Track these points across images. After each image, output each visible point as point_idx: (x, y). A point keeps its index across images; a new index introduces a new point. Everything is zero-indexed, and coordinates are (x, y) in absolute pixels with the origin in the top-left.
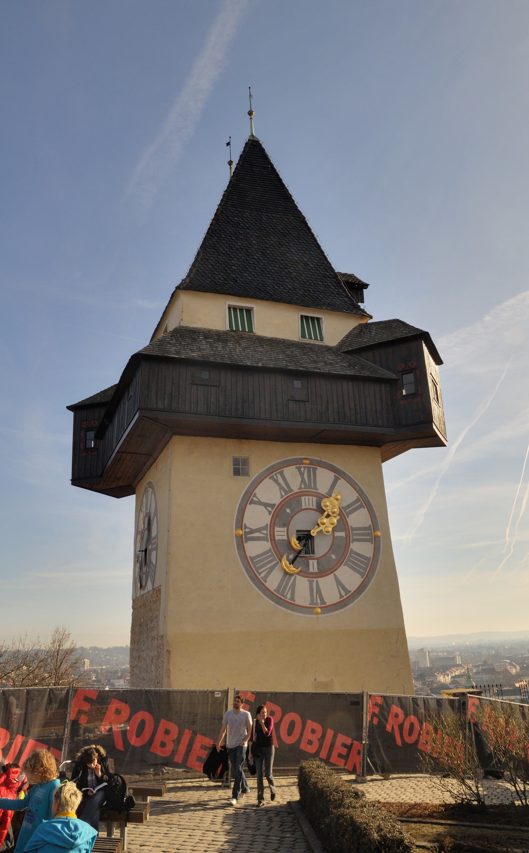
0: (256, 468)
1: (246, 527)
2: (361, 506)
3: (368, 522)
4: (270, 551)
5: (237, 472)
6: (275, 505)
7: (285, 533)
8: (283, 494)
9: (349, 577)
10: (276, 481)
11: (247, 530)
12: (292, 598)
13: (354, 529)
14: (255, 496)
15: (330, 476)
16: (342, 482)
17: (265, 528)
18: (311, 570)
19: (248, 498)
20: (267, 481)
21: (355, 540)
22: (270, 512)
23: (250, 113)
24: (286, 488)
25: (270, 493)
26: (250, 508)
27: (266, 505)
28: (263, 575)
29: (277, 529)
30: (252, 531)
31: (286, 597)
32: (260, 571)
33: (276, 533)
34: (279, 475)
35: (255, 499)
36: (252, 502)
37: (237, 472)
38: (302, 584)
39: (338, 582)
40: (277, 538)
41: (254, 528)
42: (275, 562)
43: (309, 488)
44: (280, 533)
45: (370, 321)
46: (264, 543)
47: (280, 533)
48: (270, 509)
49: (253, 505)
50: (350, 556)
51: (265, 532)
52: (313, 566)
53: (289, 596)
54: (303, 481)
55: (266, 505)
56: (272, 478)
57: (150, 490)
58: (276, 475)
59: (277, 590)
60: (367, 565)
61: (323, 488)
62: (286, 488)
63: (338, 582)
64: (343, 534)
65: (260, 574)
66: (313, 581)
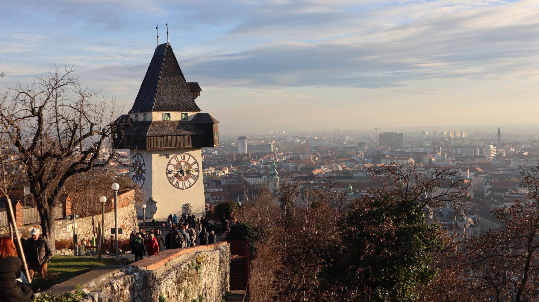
0: (171, 156)
5: (166, 158)
9: (192, 181)
15: (188, 156)
16: (191, 158)
19: (169, 164)
20: (173, 159)
23: (167, 33)
24: (177, 161)
25: (174, 162)
26: (169, 166)
37: (166, 158)
38: (181, 183)
39: (189, 182)
43: (183, 159)
45: (200, 112)
52: (183, 179)
57: (140, 156)
61: (186, 160)
62: (177, 161)
63: (189, 182)
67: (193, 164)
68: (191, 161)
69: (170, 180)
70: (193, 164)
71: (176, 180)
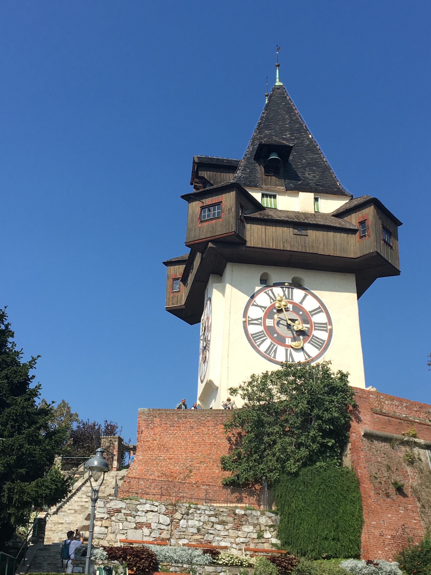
1: (249, 318)
2: (321, 311)
3: (325, 320)
4: (262, 331)
6: (266, 307)
7: (272, 323)
8: (272, 301)
10: (268, 295)
11: (250, 319)
12: (274, 357)
13: (315, 323)
14: (255, 301)
16: (309, 297)
17: (261, 319)
18: (287, 343)
21: (315, 329)
22: (263, 311)
27: (261, 307)
28: (258, 344)
29: (267, 320)
30: (253, 320)
31: (271, 356)
32: (256, 342)
33: (267, 322)
34: (270, 291)
35: (255, 303)
36: (253, 305)
40: (267, 325)
41: (254, 318)
42: (265, 338)
44: (270, 322)
46: (260, 326)
47: (270, 322)
48: (263, 309)
49: (253, 307)
50: (312, 338)
51: (260, 321)
53: (273, 356)
54: (285, 295)
55: (261, 307)
56: (266, 292)
58: (268, 291)
59: (266, 352)
60: (323, 344)
64: (308, 326)
65: (256, 343)
66: (288, 349)
67: (316, 311)
68: (310, 304)
69: (253, 340)
70: (316, 311)
71: (268, 342)
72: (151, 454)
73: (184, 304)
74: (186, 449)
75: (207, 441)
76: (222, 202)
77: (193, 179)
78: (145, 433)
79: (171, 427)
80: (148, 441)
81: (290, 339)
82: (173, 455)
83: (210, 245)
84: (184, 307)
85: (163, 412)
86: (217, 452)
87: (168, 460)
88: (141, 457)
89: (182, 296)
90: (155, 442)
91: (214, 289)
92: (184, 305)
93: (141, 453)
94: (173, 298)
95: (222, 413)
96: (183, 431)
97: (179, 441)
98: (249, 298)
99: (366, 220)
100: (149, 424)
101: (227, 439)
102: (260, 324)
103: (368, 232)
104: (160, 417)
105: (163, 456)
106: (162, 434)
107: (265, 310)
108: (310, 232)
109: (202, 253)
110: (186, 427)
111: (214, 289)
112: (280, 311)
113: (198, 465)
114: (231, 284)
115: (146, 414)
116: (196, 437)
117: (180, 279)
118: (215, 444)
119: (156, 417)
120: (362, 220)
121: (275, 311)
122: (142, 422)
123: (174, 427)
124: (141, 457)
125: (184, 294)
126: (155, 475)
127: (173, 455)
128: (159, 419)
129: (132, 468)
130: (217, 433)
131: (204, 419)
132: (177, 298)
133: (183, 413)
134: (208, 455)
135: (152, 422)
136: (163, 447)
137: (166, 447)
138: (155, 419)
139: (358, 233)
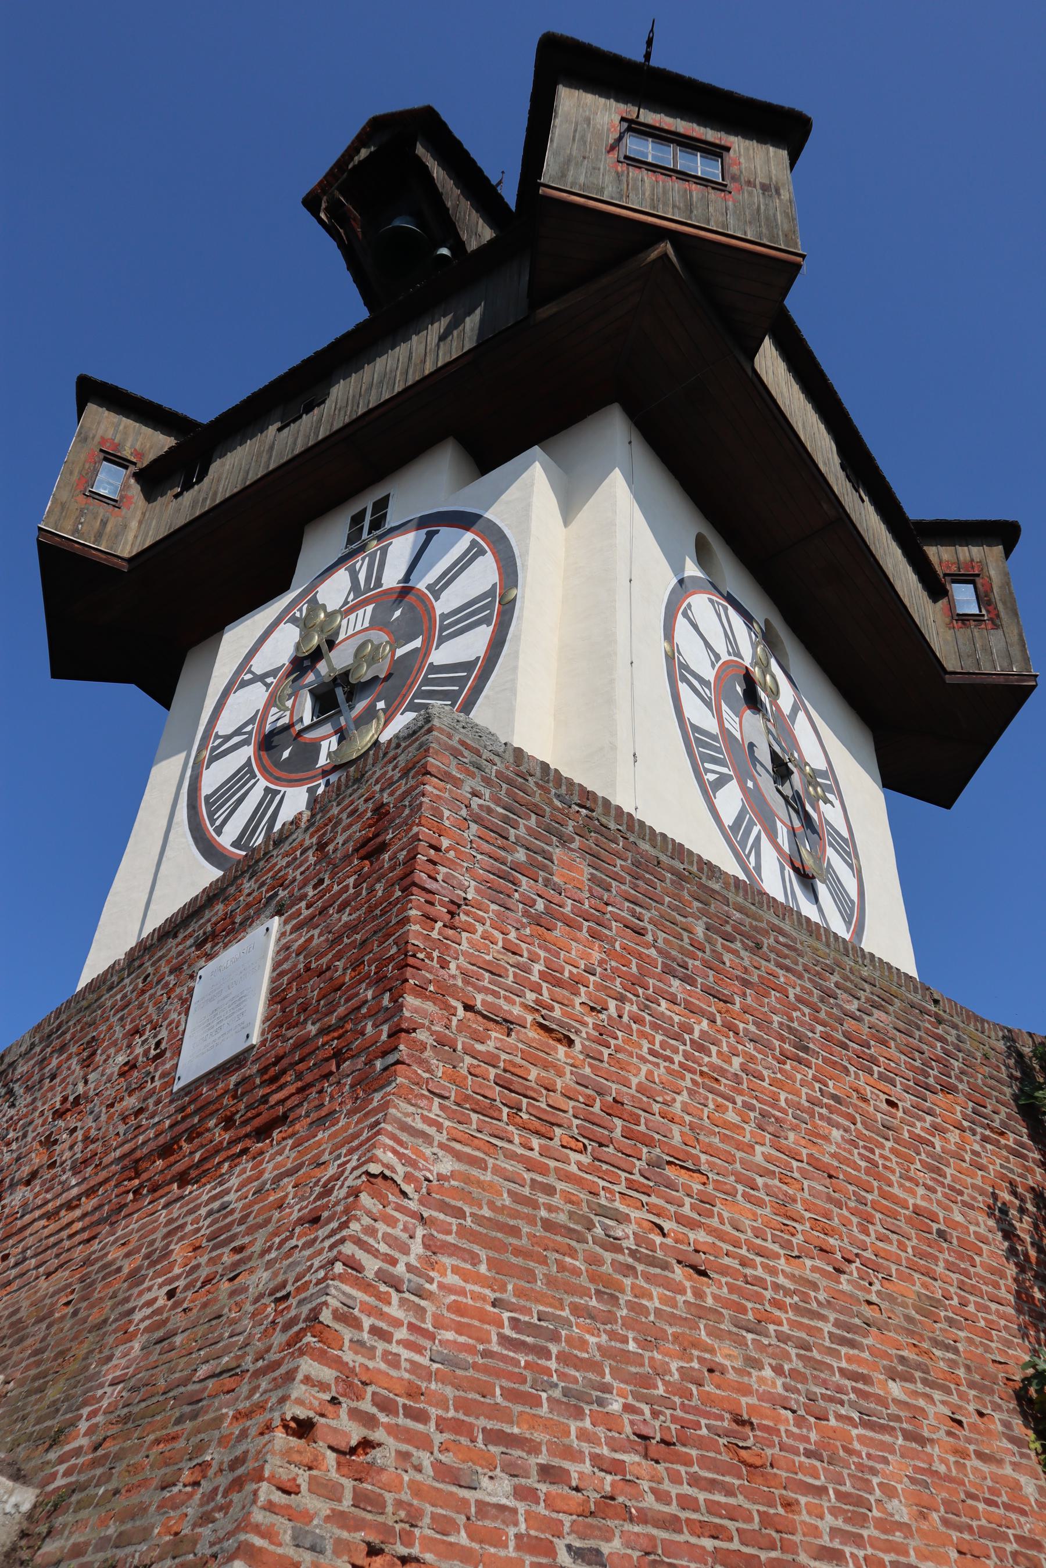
10: (719, 616)
14: (689, 606)
36: (685, 615)
72: (531, 1166)
73: (126, 554)
74: (783, 1206)
75: (896, 1190)
76: (728, 149)
77: (324, 185)
78: (481, 937)
79: (668, 971)
80: (508, 1024)
81: (785, 830)
82: (700, 1236)
83: (668, 247)
84: (125, 567)
85: (613, 826)
86: (964, 1304)
87: (679, 1273)
88: (447, 1165)
89: (125, 526)
90: (562, 1050)
91: (537, 464)
92: (130, 560)
93: (435, 1110)
94: (82, 513)
95: (940, 1021)
96: (750, 1047)
97: (731, 1116)
98: (675, 581)
99: (978, 575)
100: (516, 867)
101: (991, 1215)
102: (707, 704)
103: (988, 612)
104: (594, 857)
105: (634, 1214)
106: (612, 1004)
107: (717, 666)
108: (866, 498)
109: (538, 297)
110: (763, 1023)
111: (537, 464)
112: (752, 700)
113: (895, 1389)
114: (630, 481)
115: (492, 771)
116: (836, 1134)
117: (132, 469)
118: (941, 1233)
119: (564, 841)
120: (954, 569)
121: (739, 689)
122: (463, 824)
123: (692, 982)
124: (447, 1165)
125: (134, 524)
126: (609, 1421)
127: (700, 1236)
128: (588, 871)
129: (371, 1266)
130: (938, 1144)
131: (853, 1006)
132: (104, 523)
133: (740, 909)
134: (929, 1307)
135: (538, 865)
136: (612, 1127)
137: (649, 1143)
138: (557, 853)
139: (945, 600)
